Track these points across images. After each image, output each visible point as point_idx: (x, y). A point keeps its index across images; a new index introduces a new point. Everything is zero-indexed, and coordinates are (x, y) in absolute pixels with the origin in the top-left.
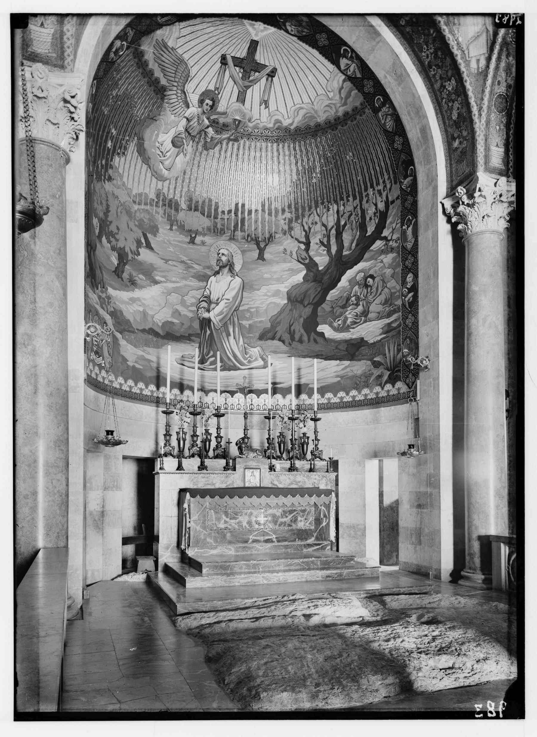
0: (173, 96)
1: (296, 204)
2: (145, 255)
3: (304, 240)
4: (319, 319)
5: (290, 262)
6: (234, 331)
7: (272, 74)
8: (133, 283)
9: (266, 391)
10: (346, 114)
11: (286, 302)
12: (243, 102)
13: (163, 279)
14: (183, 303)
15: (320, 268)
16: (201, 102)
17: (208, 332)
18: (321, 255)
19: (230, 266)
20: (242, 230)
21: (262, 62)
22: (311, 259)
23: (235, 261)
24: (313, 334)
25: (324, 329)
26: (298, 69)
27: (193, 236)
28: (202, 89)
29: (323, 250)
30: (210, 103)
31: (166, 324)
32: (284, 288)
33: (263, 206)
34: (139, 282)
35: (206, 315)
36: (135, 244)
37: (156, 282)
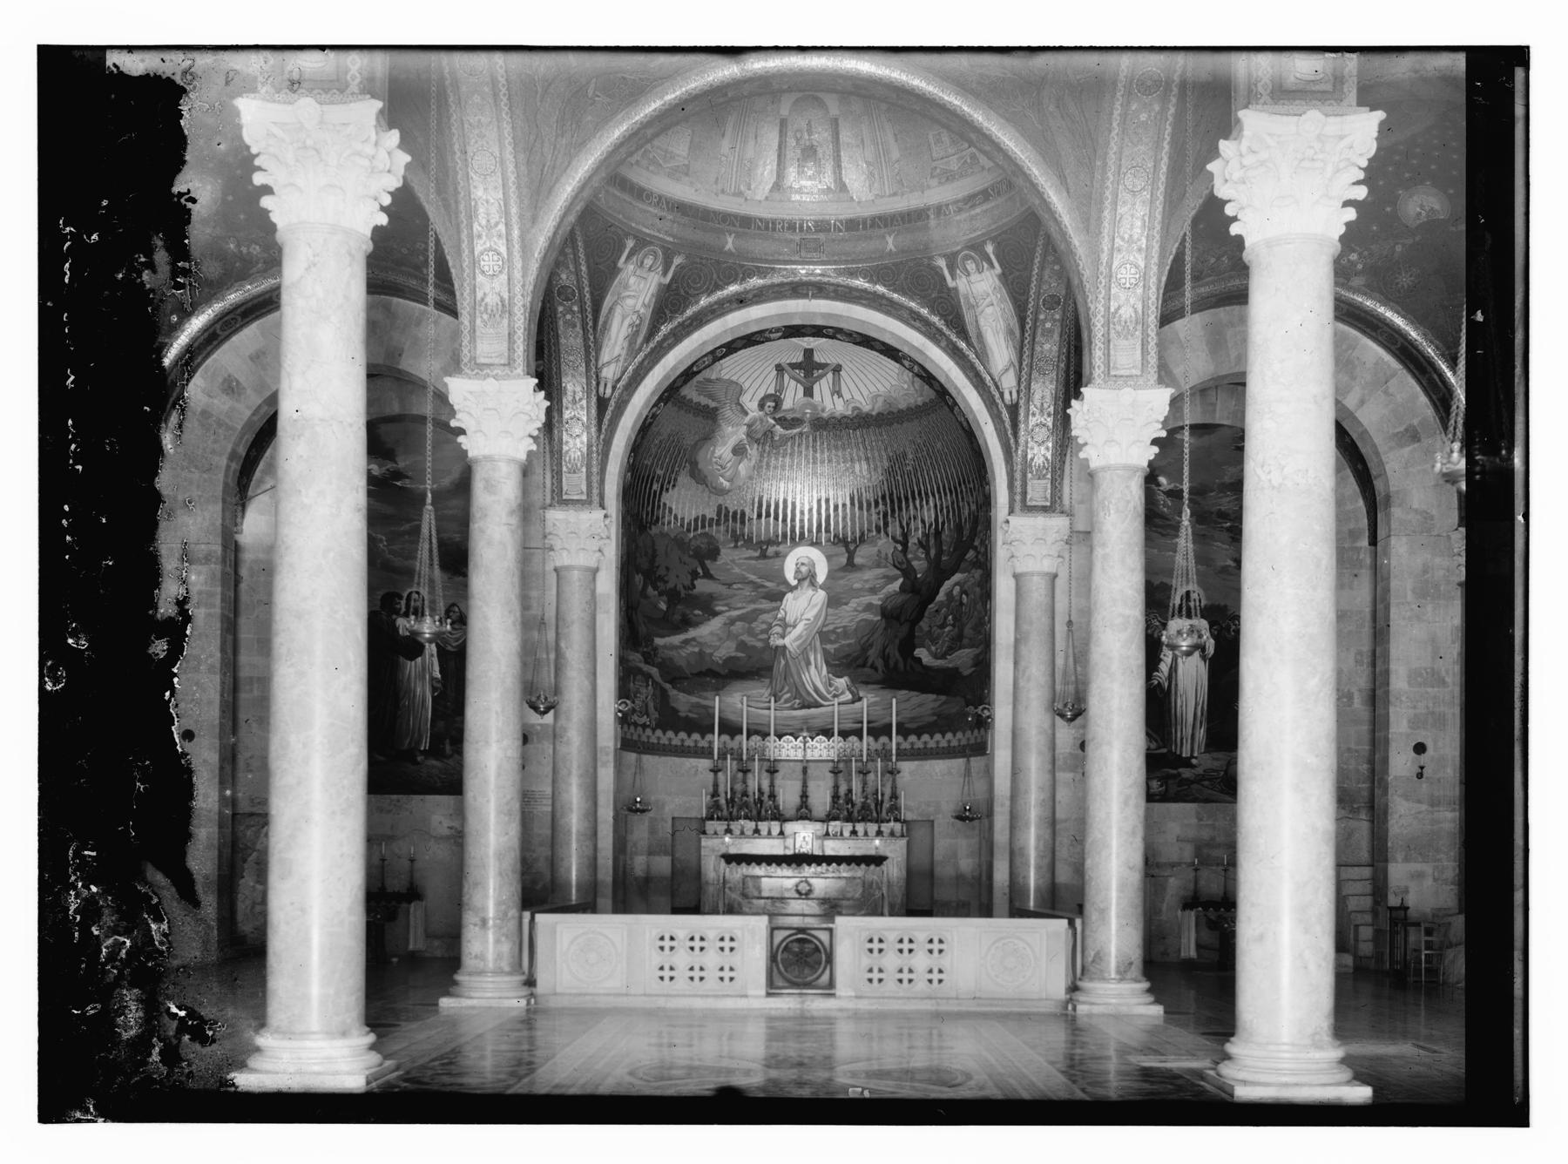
0: (728, 412)
1: (891, 495)
2: (703, 586)
3: (901, 539)
4: (917, 641)
5: (885, 567)
6: (815, 659)
7: (837, 369)
8: (686, 623)
10: (925, 404)
11: (879, 618)
12: (811, 396)
13: (726, 608)
14: (751, 632)
15: (919, 576)
16: (761, 406)
17: (783, 662)
18: (918, 559)
20: (828, 531)
21: (823, 361)
22: (909, 562)
23: (818, 570)
24: (909, 660)
25: (922, 653)
26: (856, 370)
27: (765, 547)
28: (761, 394)
29: (921, 554)
30: (773, 404)
31: (730, 659)
32: (876, 600)
33: (852, 499)
34: (694, 618)
35: (780, 642)
36: (689, 577)
37: (715, 614)
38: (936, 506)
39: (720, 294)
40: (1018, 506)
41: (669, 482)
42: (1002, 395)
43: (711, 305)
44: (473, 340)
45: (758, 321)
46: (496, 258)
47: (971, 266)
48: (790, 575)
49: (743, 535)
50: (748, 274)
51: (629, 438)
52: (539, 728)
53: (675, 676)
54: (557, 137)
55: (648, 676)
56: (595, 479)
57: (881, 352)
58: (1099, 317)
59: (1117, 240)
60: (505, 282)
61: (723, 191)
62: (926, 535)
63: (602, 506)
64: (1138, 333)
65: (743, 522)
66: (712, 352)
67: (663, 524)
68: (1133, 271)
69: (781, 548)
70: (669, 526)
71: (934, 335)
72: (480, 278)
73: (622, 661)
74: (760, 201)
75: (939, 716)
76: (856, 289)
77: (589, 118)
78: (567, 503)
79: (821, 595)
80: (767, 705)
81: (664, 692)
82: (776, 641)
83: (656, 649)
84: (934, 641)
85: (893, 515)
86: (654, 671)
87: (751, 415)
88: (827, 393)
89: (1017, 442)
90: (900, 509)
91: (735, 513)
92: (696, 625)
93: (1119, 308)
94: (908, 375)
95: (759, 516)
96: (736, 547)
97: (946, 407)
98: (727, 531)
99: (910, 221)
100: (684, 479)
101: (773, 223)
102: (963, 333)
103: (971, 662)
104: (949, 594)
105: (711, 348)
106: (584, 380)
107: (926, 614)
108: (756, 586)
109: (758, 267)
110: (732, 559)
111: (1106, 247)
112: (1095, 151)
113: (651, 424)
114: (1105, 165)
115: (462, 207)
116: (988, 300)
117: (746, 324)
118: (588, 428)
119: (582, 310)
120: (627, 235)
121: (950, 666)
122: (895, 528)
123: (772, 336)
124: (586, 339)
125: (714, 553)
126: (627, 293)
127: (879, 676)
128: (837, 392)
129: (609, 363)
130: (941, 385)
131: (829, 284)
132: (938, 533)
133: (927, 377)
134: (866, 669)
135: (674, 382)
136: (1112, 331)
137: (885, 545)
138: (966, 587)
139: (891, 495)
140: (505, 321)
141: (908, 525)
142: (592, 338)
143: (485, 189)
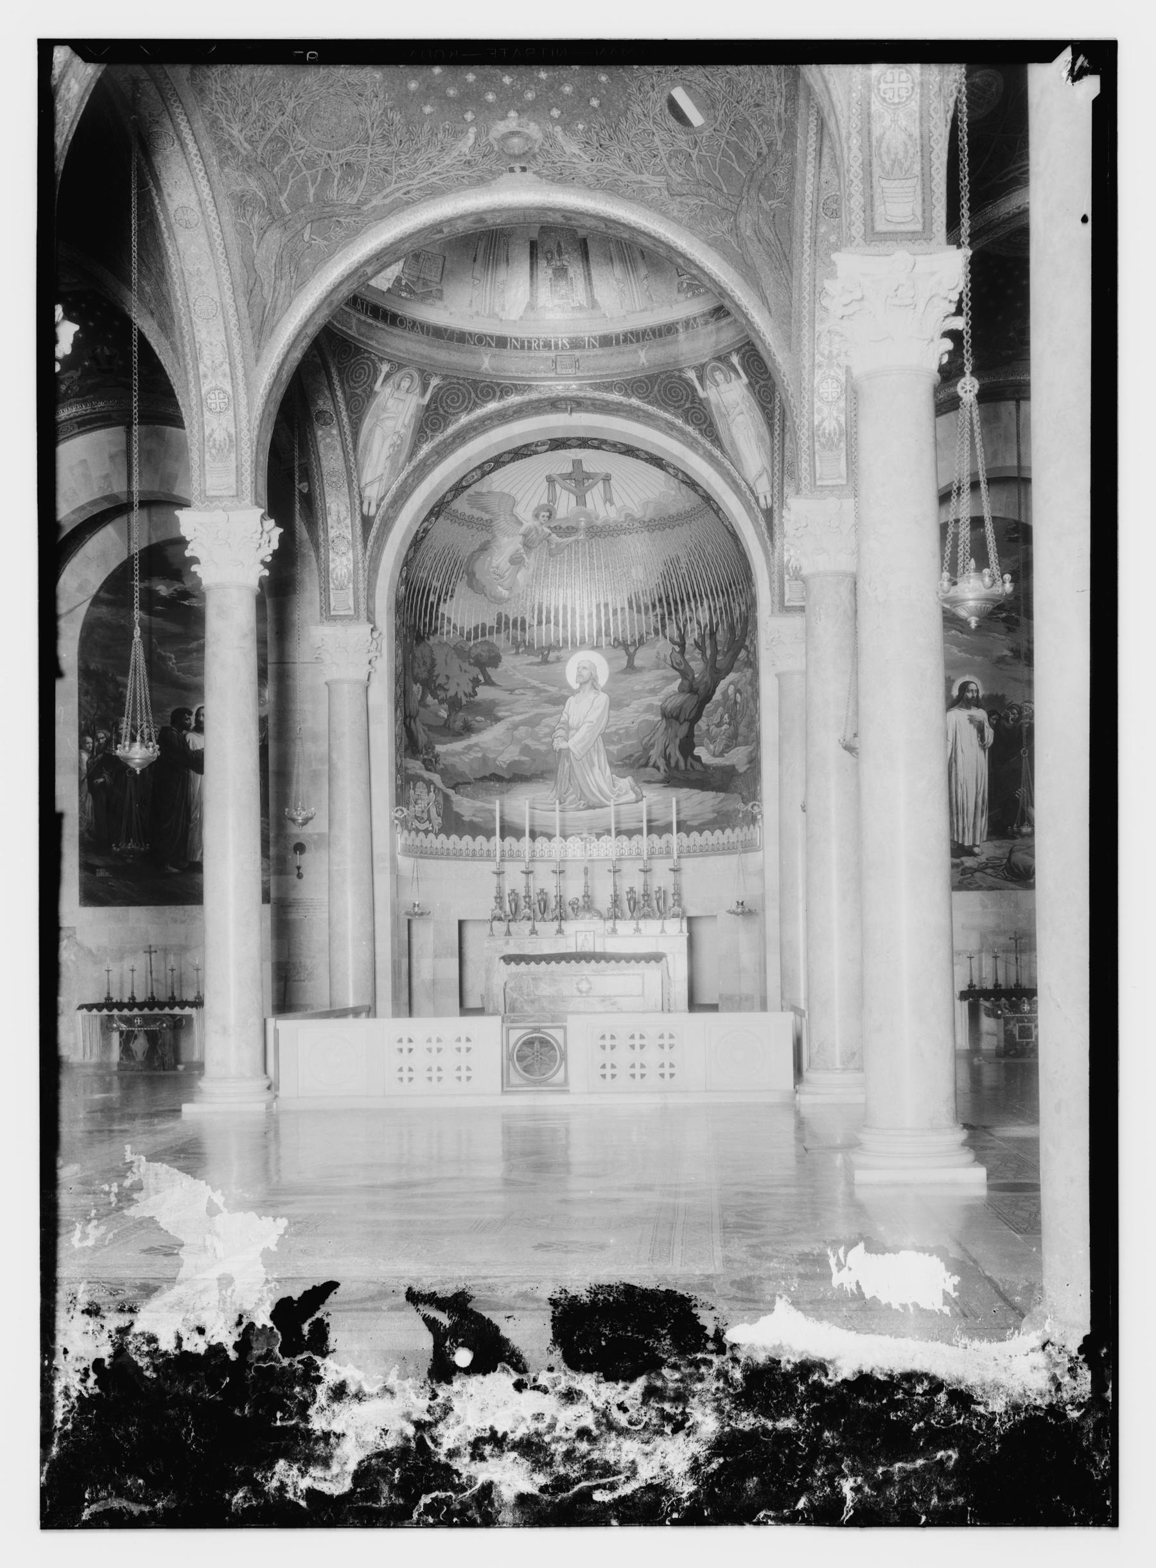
0: (502, 523)
1: (667, 597)
2: (484, 693)
3: (678, 640)
4: (696, 740)
5: (664, 668)
7: (607, 479)
8: (468, 729)
9: (639, 831)
12: (585, 504)
16: (536, 516)
17: (567, 764)
18: (694, 659)
19: (592, 681)
20: (607, 635)
28: (534, 504)
29: (697, 654)
31: (513, 764)
32: (656, 701)
33: (630, 603)
34: (476, 725)
35: (563, 745)
36: (471, 685)
37: (498, 720)
38: (710, 607)
39: (479, 412)
40: (777, 606)
41: (447, 594)
42: (757, 499)
43: (471, 423)
44: (203, 474)
45: (521, 435)
46: (222, 396)
47: (719, 376)
48: (572, 679)
49: (524, 641)
50: (505, 391)
51: (399, 553)
52: (316, 837)
53: (458, 782)
54: (276, 278)
55: (429, 783)
56: (362, 594)
57: (646, 460)
58: (804, 430)
59: (817, 357)
60: (232, 420)
61: (477, 313)
62: (702, 636)
63: (371, 619)
64: (843, 445)
65: (523, 629)
66: (479, 467)
67: (442, 634)
68: (835, 385)
69: (562, 653)
70: (447, 636)
71: (692, 445)
72: (207, 415)
73: (400, 769)
74: (515, 322)
75: (718, 813)
76: (613, 403)
77: (307, 260)
78: (335, 618)
79: (603, 699)
80: (551, 807)
81: (446, 797)
82: (559, 744)
83: (437, 756)
84: (713, 740)
85: (670, 619)
86: (436, 778)
87: (526, 525)
88: (599, 501)
89: (773, 545)
90: (676, 610)
91: (515, 621)
92: (478, 731)
93: (823, 421)
94: (674, 483)
95: (540, 623)
96: (517, 653)
97: (711, 512)
98: (508, 638)
99: (660, 336)
100: (461, 588)
101: (529, 342)
102: (716, 440)
103: (745, 760)
104: (725, 694)
105: (478, 463)
106: (348, 500)
107: (704, 713)
108: (538, 691)
109: (515, 385)
110: (513, 666)
111: (807, 364)
112: (791, 273)
113: (423, 538)
114: (800, 286)
115: (187, 350)
116: (738, 410)
117: (509, 439)
118: (354, 547)
119: (341, 433)
120: (381, 360)
121: (728, 763)
122: (672, 631)
123: (539, 449)
124: (347, 460)
125: (495, 660)
126: (386, 415)
127: (660, 775)
128: (609, 500)
129: (372, 482)
130: (705, 491)
131: (585, 398)
132: (713, 634)
133: (691, 484)
134: (648, 769)
135: (444, 497)
136: (817, 444)
137: (663, 647)
138: (739, 687)
139: (667, 597)
140: (233, 456)
141: (685, 626)
142: (352, 459)
143: (208, 333)
